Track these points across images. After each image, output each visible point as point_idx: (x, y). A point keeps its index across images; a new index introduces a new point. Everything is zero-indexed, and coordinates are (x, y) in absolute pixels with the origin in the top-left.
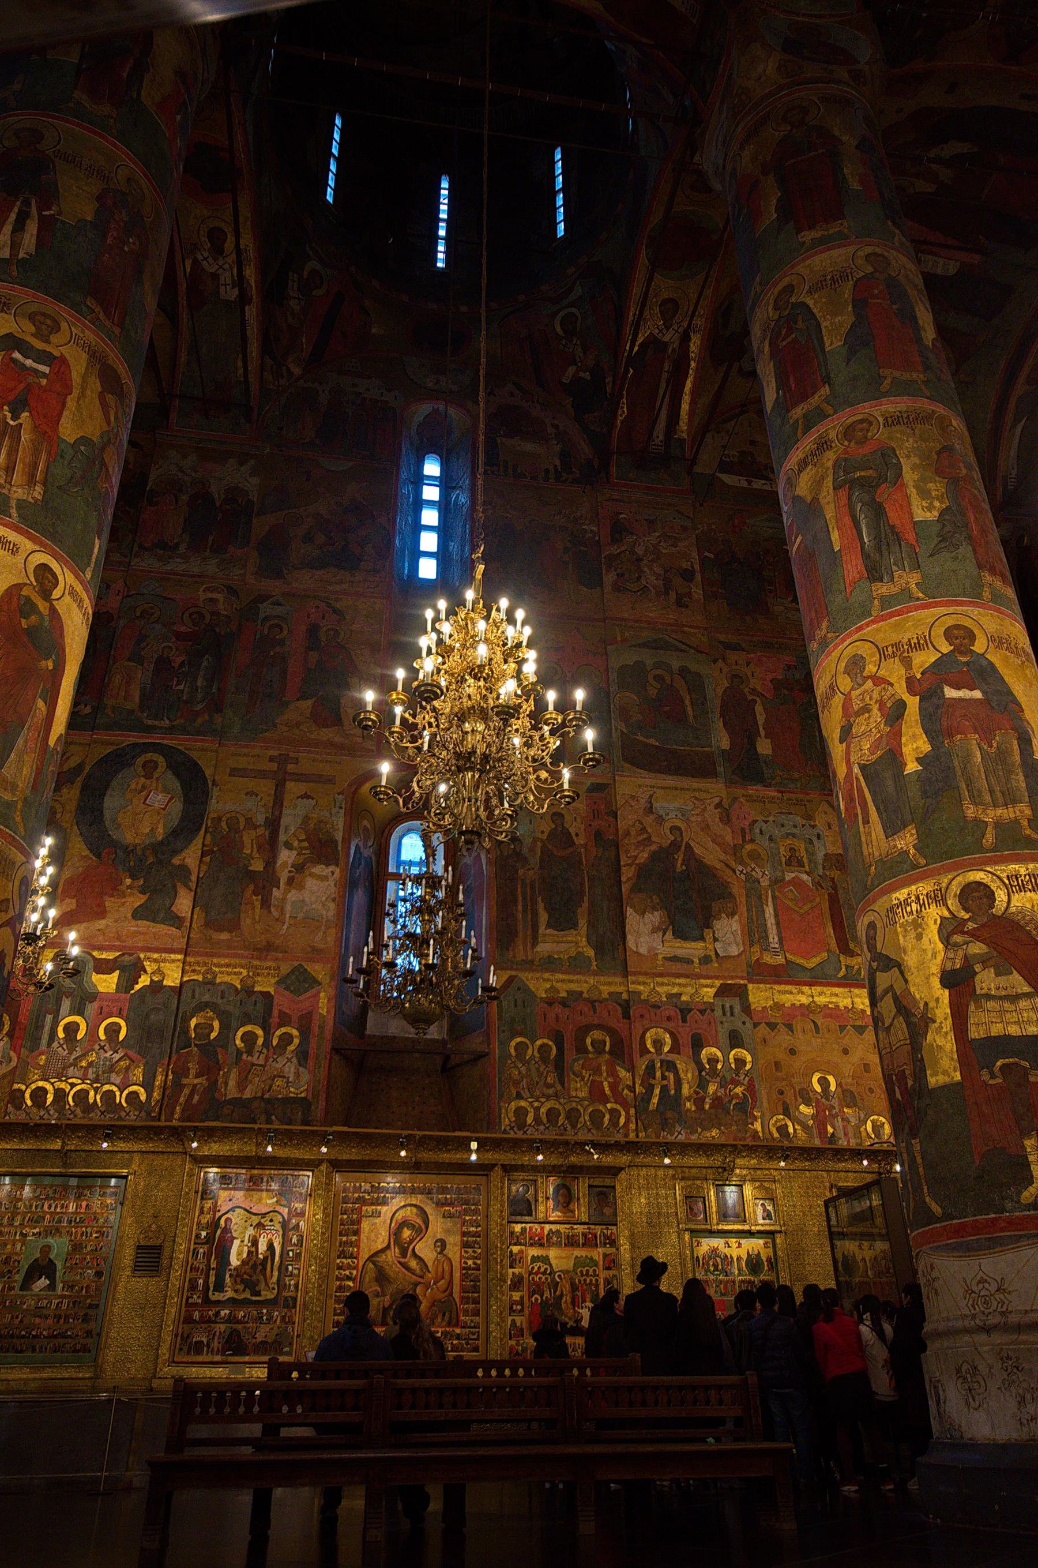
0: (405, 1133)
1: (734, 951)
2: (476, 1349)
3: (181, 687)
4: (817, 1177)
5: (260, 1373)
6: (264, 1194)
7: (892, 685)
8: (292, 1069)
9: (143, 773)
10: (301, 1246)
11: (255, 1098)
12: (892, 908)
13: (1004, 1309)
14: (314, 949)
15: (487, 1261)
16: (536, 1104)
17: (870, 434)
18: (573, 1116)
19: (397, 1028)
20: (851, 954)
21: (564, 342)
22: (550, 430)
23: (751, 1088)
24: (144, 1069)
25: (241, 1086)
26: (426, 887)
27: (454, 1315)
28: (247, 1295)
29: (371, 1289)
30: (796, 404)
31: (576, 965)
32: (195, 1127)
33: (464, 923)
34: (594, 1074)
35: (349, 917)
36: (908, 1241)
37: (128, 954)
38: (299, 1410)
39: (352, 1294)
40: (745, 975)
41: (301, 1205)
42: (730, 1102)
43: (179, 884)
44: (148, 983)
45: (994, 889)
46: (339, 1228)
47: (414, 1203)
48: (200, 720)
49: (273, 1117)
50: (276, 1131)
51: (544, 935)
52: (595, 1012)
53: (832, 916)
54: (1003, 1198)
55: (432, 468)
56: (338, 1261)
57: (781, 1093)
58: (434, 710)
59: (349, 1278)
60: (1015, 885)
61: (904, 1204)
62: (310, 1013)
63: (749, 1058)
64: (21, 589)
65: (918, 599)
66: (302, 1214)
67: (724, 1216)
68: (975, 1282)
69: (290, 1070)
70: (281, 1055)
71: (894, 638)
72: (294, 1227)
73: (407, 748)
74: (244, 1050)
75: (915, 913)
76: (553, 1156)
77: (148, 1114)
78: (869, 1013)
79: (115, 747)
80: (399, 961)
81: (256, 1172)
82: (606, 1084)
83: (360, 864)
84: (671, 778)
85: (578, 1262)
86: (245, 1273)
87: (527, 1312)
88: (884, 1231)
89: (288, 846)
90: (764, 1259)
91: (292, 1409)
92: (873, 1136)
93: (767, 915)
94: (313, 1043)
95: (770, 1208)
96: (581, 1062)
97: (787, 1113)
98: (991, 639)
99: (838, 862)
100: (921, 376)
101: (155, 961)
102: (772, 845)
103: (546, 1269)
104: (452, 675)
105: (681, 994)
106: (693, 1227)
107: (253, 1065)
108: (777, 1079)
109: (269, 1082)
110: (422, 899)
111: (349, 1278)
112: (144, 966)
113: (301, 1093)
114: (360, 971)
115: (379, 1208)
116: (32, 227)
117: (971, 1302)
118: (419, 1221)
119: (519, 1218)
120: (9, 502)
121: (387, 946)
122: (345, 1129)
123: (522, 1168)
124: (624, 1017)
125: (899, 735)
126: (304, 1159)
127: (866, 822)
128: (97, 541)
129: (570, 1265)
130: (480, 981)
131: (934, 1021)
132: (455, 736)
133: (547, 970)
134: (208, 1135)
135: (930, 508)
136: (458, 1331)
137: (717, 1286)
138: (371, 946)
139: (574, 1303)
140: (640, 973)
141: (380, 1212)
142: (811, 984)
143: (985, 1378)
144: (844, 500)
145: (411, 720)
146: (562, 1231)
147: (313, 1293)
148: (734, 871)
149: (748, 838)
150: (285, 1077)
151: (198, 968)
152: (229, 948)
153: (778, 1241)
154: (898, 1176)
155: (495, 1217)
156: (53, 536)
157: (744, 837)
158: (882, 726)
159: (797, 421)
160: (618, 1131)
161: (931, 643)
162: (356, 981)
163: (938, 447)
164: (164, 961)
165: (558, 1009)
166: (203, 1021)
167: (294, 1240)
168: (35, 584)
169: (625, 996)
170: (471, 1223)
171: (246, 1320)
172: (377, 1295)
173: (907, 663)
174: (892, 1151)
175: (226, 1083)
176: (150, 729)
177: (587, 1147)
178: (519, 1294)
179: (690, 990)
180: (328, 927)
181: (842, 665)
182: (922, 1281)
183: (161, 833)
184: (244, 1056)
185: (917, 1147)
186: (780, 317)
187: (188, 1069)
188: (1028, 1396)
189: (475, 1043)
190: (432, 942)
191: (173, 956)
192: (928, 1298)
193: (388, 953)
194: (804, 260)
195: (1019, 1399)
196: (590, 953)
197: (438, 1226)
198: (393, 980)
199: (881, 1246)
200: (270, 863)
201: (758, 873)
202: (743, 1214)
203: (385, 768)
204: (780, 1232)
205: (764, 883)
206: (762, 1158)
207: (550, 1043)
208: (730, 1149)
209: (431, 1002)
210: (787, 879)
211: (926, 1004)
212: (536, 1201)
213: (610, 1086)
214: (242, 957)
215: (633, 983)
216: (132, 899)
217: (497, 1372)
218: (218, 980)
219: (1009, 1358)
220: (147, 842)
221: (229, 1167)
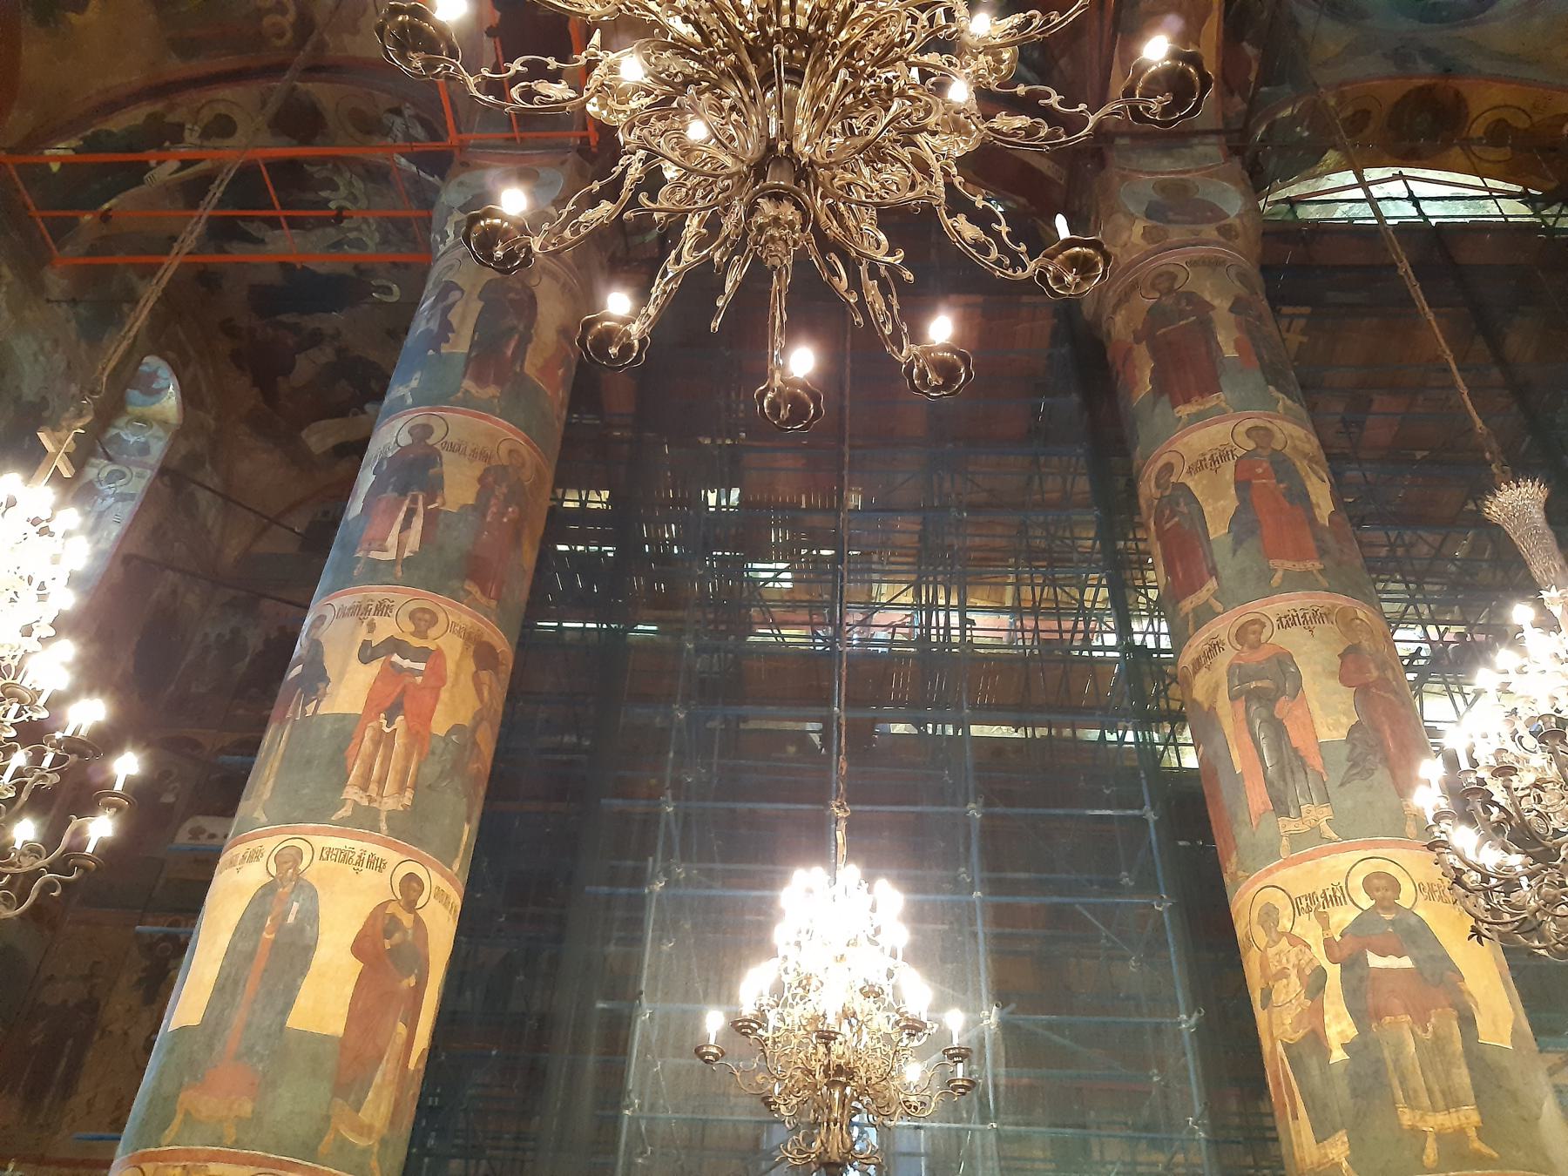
7: (1309, 947)
30: (1185, 596)
64: (386, 908)
65: (1330, 840)
98: (1419, 888)
100: (1318, 565)
116: (418, 523)
120: (379, 816)
125: (1319, 1011)
127: (1295, 1117)
156: (419, 842)
159: (1187, 614)
168: (400, 897)
173: (1324, 921)
181: (1255, 915)
186: (1162, 497)
194: (1182, 437)
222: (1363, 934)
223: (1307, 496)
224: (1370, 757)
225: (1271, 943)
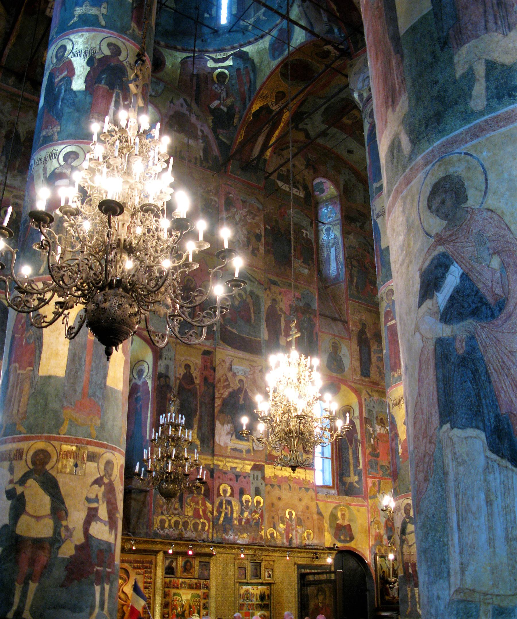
16: (170, 518)
18: (185, 524)
21: (216, 86)
22: (200, 133)
23: (262, 516)
40: (264, 460)
57: (273, 518)
63: (262, 501)
82: (201, 510)
84: (241, 352)
97: (274, 527)
108: (272, 511)
169: (212, 466)
179: (241, 466)
215: (217, 460)
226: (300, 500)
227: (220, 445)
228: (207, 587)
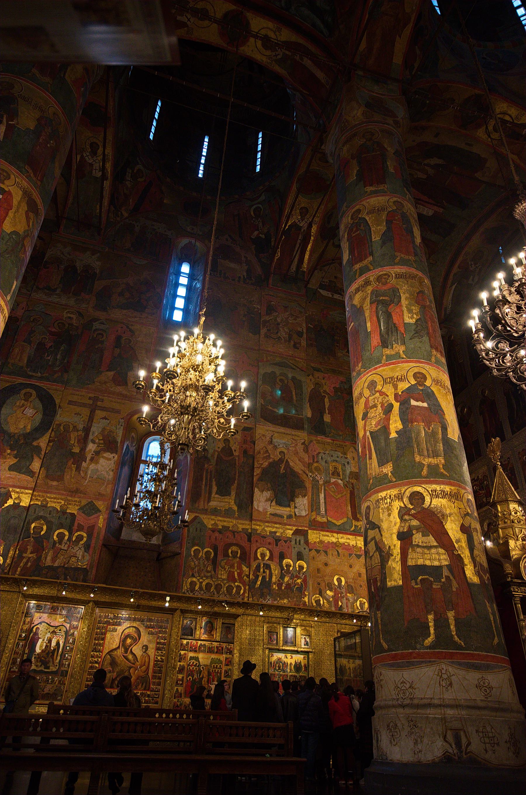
0: (134, 590)
1: (304, 513)
2: (157, 703)
3: (49, 358)
4: (331, 626)
5: (43, 710)
6: (58, 616)
7: (388, 396)
8: (81, 553)
9: (23, 398)
10: (74, 644)
11: (59, 567)
12: (378, 500)
13: (412, 696)
14: (100, 494)
15: (167, 658)
16: (201, 580)
17: (388, 281)
18: (218, 588)
19: (137, 537)
20: (358, 520)
22: (243, 259)
23: (305, 581)
24: (4, 547)
25: (53, 560)
26: (159, 469)
27: (148, 684)
28: (42, 668)
29: (107, 668)
30: (356, 263)
31: (228, 513)
32: (26, 579)
33: (176, 488)
34: (231, 567)
35: (119, 480)
36: (371, 659)
37: (3, 488)
38: (62, 730)
39: (98, 671)
40: (308, 525)
41: (77, 623)
42: (294, 586)
43: (35, 455)
44: (12, 503)
45: (425, 496)
46: (95, 636)
47: (135, 625)
48: (56, 375)
49: (68, 577)
50: (69, 584)
51: (214, 497)
52: (234, 537)
53: (351, 502)
54: (416, 643)
55: (185, 268)
56: (92, 653)
57: (319, 584)
58: (173, 383)
59: (96, 662)
60: (434, 494)
61: (371, 642)
62: (93, 526)
63: (305, 566)
65: (403, 358)
66: (77, 628)
67: (286, 643)
68: (399, 683)
69: (80, 554)
70: (76, 546)
71: (391, 375)
72: (71, 635)
73: (158, 400)
74: (57, 542)
75: (388, 503)
76: (206, 607)
77: (3, 571)
78: (363, 549)
79: (11, 384)
80: (142, 504)
81: (55, 604)
82: (236, 573)
83: (127, 455)
84: (282, 428)
85: (213, 661)
86: (43, 657)
87: (184, 685)
88: (360, 655)
89: (93, 442)
90: (303, 665)
91: (58, 730)
92: (360, 608)
93: (321, 498)
94: (93, 541)
95: (308, 640)
96: (225, 561)
97: (320, 594)
98: (433, 380)
99: (356, 476)
101: (17, 492)
102: (327, 465)
103: (197, 663)
104: (184, 368)
105: (276, 532)
106: (270, 647)
107: (61, 549)
108: (318, 577)
109: (68, 559)
110: (156, 474)
111: (96, 662)
112: (11, 495)
113: (84, 565)
114: (121, 507)
115: (116, 627)
117: (397, 692)
118: (136, 636)
119: (186, 637)
121: (136, 496)
122: (104, 586)
123: (191, 612)
124: (248, 541)
126: (81, 599)
127: (370, 458)
128: (15, 282)
129: (208, 662)
130: (180, 517)
131: (392, 555)
132: (181, 397)
133: (213, 515)
134: (32, 584)
135: (412, 318)
136: (149, 693)
137: (279, 677)
138: (128, 495)
139: (209, 681)
140: (258, 520)
141: (117, 629)
142: (338, 533)
143: (400, 730)
144: (374, 309)
145: (161, 387)
146: (207, 645)
147: (77, 670)
148: (307, 475)
149: (315, 460)
150: (77, 557)
151: (39, 498)
152: (57, 489)
153: (310, 656)
154: (369, 628)
155: (174, 636)
157: (314, 460)
158: (382, 414)
160: (239, 597)
161: (407, 379)
162: (119, 512)
163: (418, 291)
164: (22, 493)
165: (217, 534)
166: (38, 525)
167: (71, 641)
169: (250, 531)
170: (162, 638)
171: (40, 681)
172: (110, 672)
173: (396, 387)
174: (368, 616)
175: (46, 558)
176: (30, 377)
177: (223, 604)
178: (182, 675)
180: (108, 484)
181: (366, 384)
182: (375, 680)
183: (29, 428)
184: (57, 545)
185: (379, 615)
186: (353, 223)
187: (27, 549)
188: (419, 740)
189: (174, 547)
190: (159, 496)
191: (27, 491)
192: (378, 689)
193: (136, 499)
195: (415, 741)
196: (235, 508)
197: (145, 639)
198: (137, 513)
199: (358, 662)
200: (83, 449)
201: (318, 478)
202: (294, 642)
203: (146, 409)
204: (312, 652)
205: (321, 482)
206: (307, 615)
207: (211, 551)
208: (292, 609)
209: (155, 525)
210: (332, 481)
211: (390, 547)
212: (196, 629)
213: (237, 574)
214: (63, 494)
215: (254, 525)
216: (9, 460)
217: (166, 715)
218: (49, 505)
219: (412, 721)
220: (21, 433)
221: (42, 601)
222: (410, 392)
223: (413, 232)
224: (423, 331)
225: (372, 395)
226: (351, 566)
227: (257, 510)
228: (230, 652)
